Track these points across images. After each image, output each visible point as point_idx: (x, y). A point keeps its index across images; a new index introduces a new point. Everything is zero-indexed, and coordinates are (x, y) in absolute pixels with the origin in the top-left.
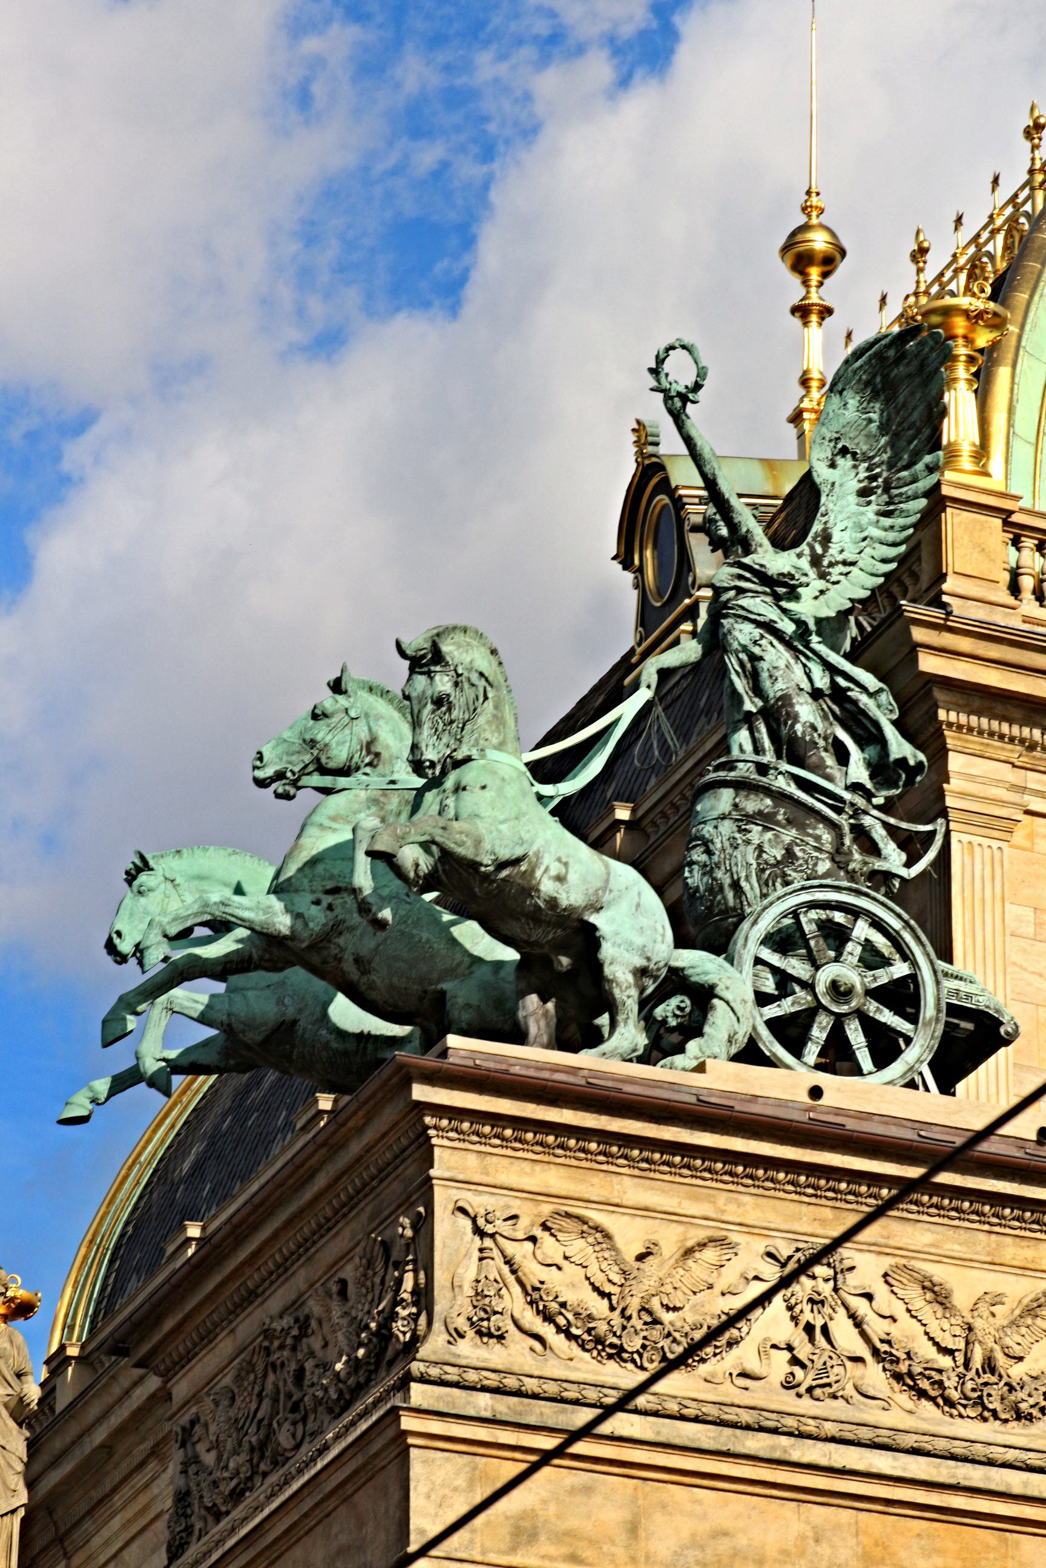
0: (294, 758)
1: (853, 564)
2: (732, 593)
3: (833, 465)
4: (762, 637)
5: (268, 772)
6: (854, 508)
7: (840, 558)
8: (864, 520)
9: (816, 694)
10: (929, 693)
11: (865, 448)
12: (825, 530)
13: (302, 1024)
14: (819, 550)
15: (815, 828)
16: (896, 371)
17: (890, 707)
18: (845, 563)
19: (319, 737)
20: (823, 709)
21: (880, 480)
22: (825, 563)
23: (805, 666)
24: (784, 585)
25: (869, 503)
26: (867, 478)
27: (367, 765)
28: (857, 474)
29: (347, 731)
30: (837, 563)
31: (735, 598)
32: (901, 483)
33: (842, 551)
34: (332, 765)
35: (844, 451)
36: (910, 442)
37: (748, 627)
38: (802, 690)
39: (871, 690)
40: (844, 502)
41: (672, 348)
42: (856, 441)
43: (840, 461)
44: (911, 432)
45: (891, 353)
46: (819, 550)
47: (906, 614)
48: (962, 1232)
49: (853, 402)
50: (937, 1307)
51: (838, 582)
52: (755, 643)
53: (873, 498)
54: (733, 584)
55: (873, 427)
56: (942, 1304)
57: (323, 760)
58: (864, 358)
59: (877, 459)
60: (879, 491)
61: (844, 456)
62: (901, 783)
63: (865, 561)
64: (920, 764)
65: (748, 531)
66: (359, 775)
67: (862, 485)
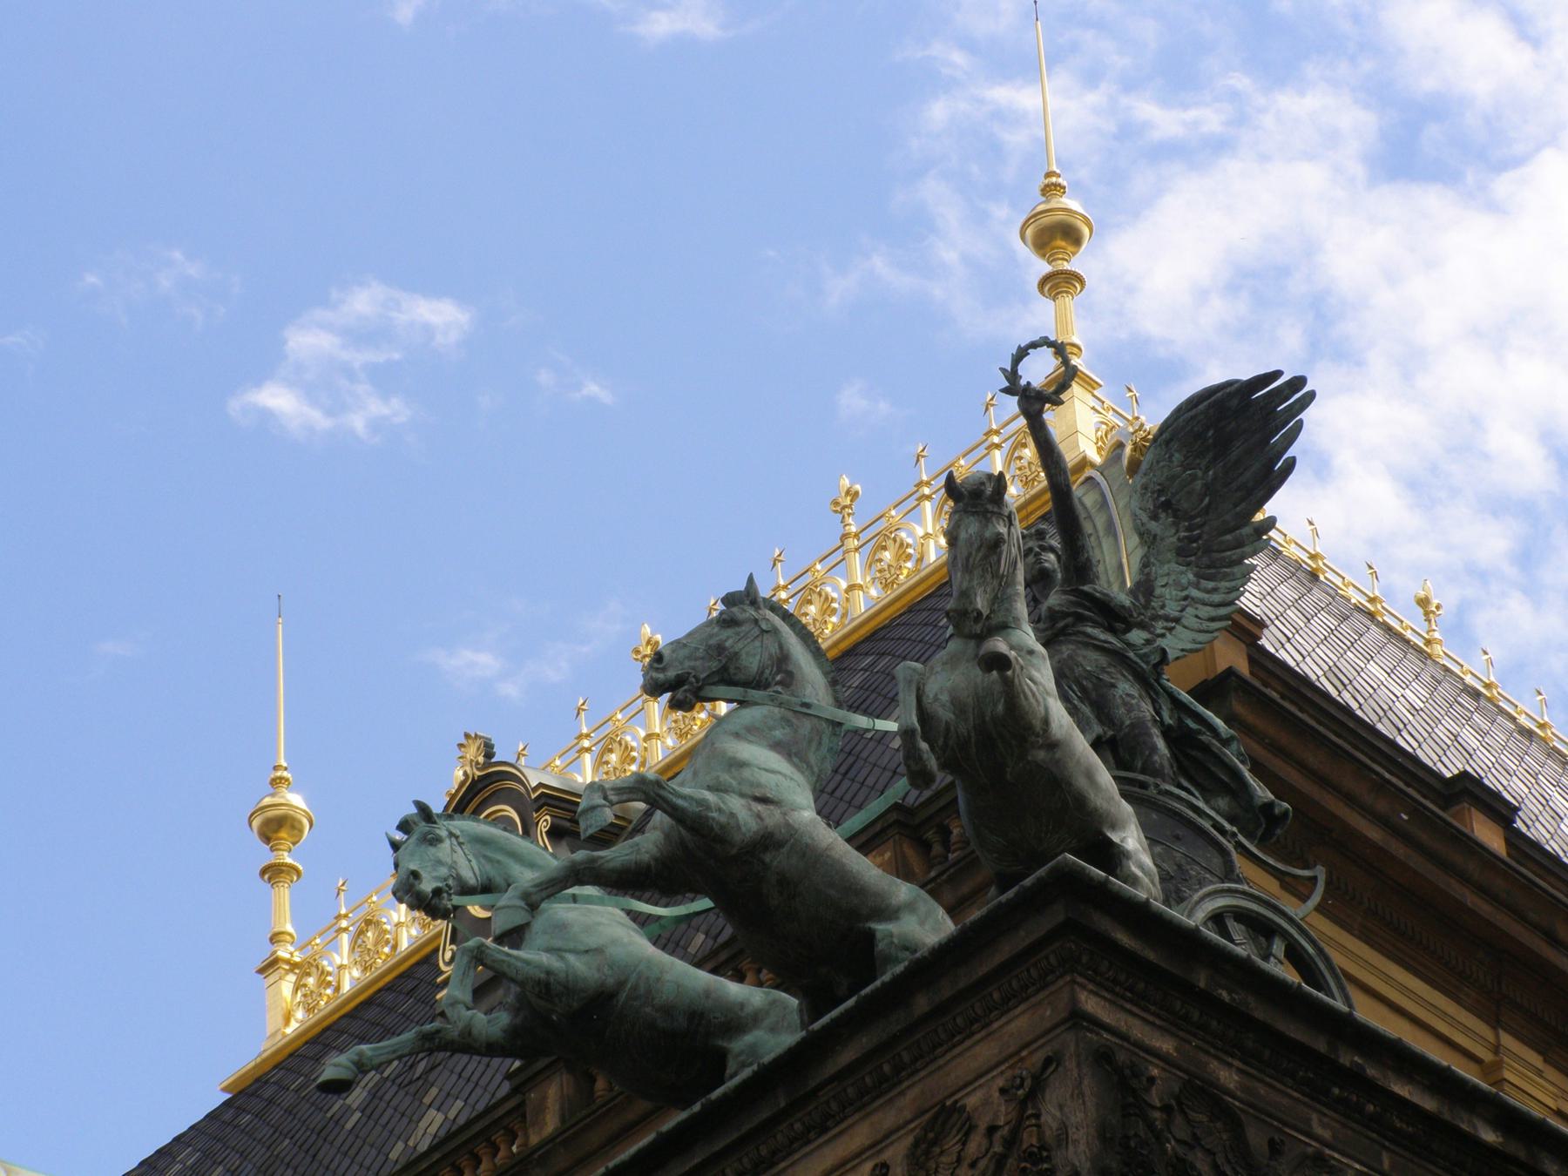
0: (698, 663)
1: (1177, 620)
2: (1070, 620)
5: (671, 674)
7: (1161, 612)
8: (1184, 581)
13: (623, 996)
16: (1233, 424)
18: (1167, 618)
19: (728, 644)
23: (1154, 702)
24: (1124, 620)
27: (778, 683)
29: (757, 643)
31: (1073, 625)
34: (740, 677)
35: (1167, 506)
36: (1236, 506)
37: (1094, 655)
41: (1034, 345)
44: (1239, 494)
45: (1235, 402)
49: (1177, 457)
51: (1163, 636)
52: (1103, 670)
54: (1072, 610)
55: (1198, 485)
57: (732, 671)
58: (1201, 407)
62: (1259, 833)
63: (1189, 618)
64: (1286, 812)
66: (769, 692)
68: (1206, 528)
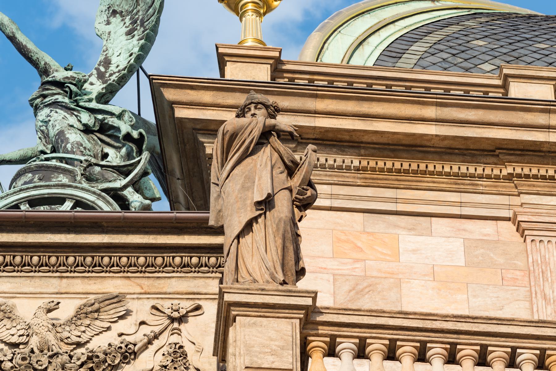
3: (108, 23)
4: (51, 111)
6: (125, 42)
9: (87, 130)
10: (197, 140)
11: (126, 8)
12: (105, 59)
14: (102, 69)
15: (57, 177)
17: (130, 119)
20: (94, 140)
21: (138, 21)
22: (107, 75)
23: (76, 116)
25: (133, 37)
26: (131, 24)
28: (125, 23)
30: (114, 73)
32: (149, 17)
33: (118, 66)
35: (114, 13)
38: (72, 126)
39: (117, 113)
40: (118, 41)
42: (121, 5)
43: (112, 20)
46: (102, 69)
47: (154, 81)
48: (37, 280)
50: (5, 321)
53: (136, 32)
56: (9, 318)
59: (135, 11)
60: (138, 28)
61: (115, 17)
62: (134, 154)
65: (45, 64)
67: (128, 29)
68: (141, 13)
